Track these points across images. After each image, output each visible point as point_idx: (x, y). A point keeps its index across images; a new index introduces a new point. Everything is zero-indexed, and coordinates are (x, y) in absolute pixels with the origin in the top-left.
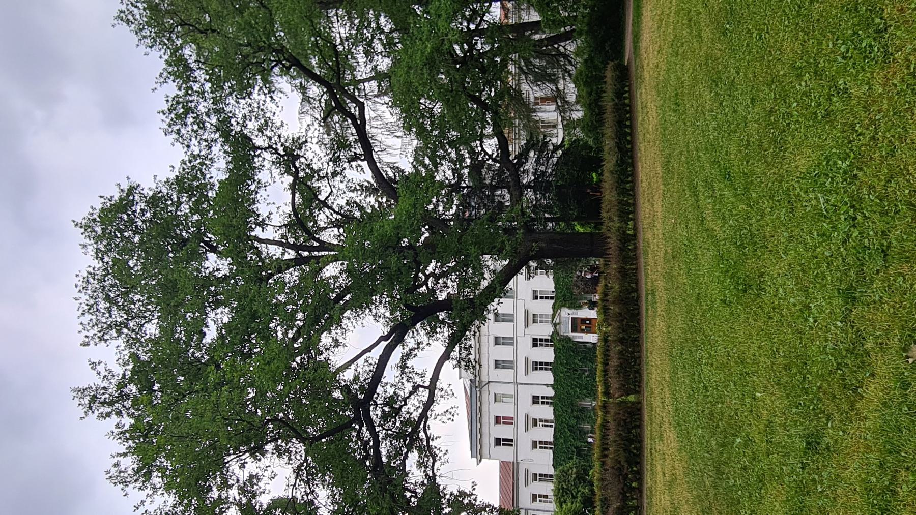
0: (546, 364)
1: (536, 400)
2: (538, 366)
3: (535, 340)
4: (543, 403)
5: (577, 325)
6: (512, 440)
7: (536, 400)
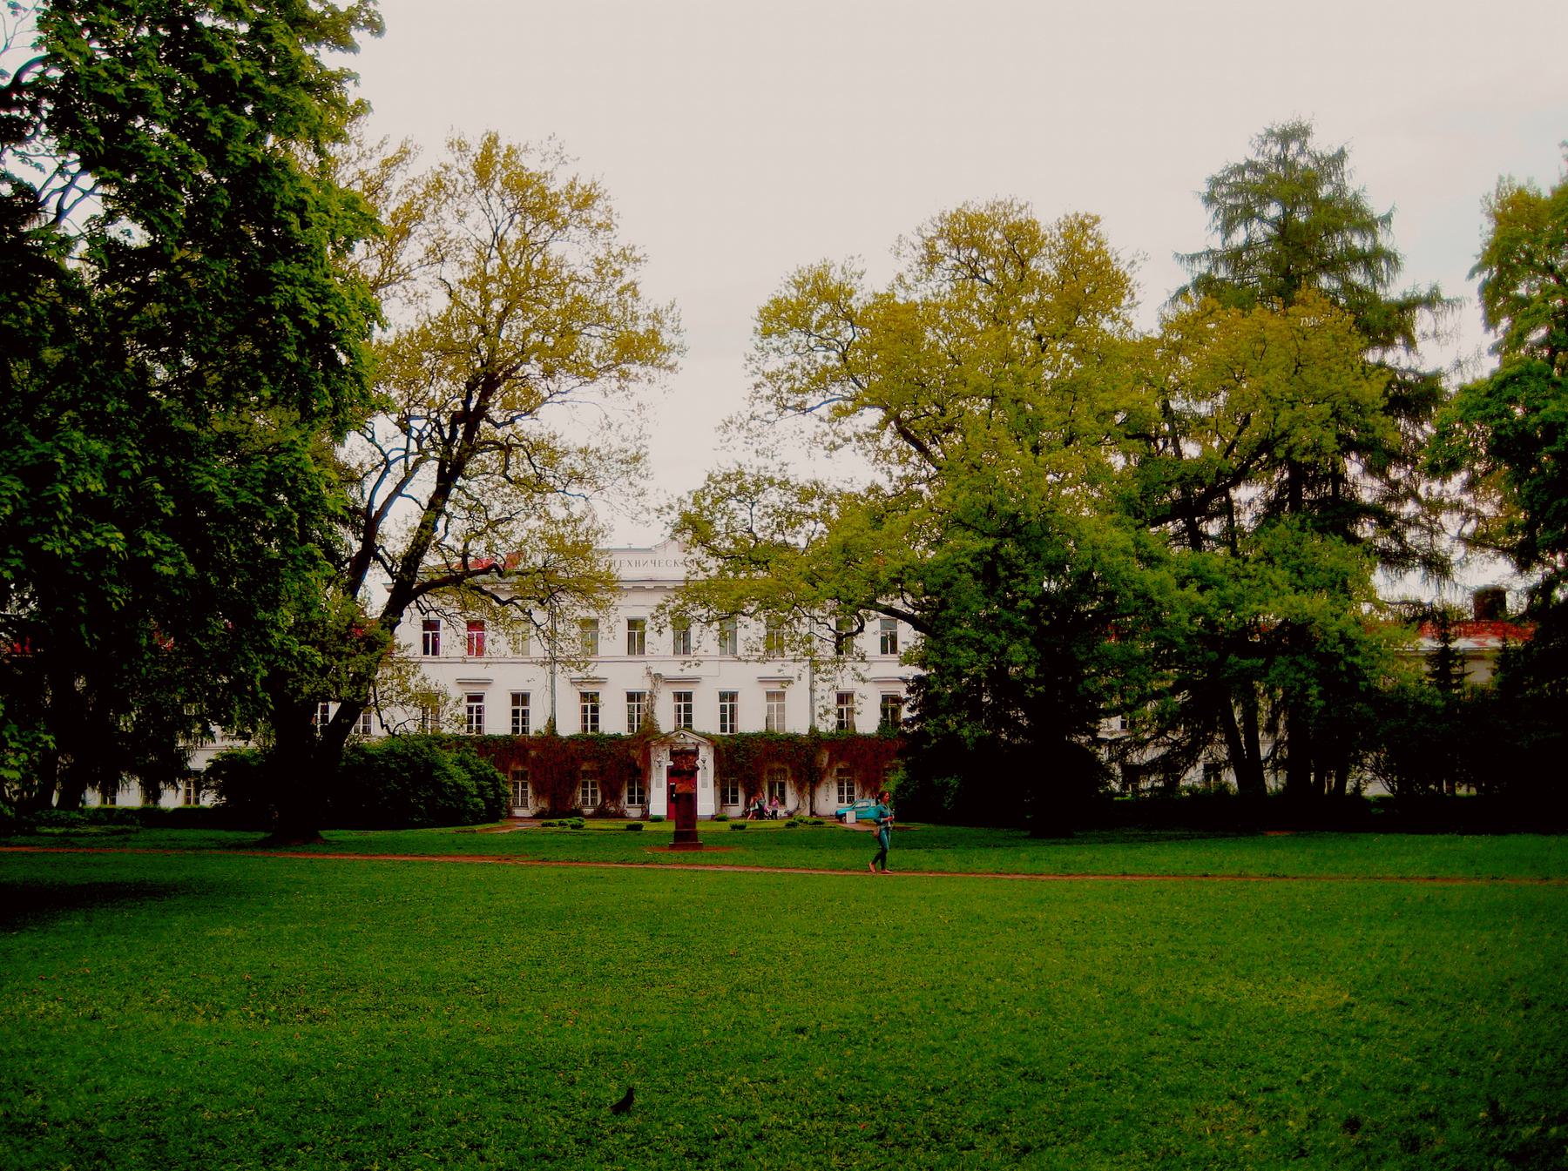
0: (595, 719)
1: (520, 699)
2: (591, 704)
3: (732, 696)
4: (515, 713)
5: (683, 772)
6: (435, 652)
7: (520, 699)
